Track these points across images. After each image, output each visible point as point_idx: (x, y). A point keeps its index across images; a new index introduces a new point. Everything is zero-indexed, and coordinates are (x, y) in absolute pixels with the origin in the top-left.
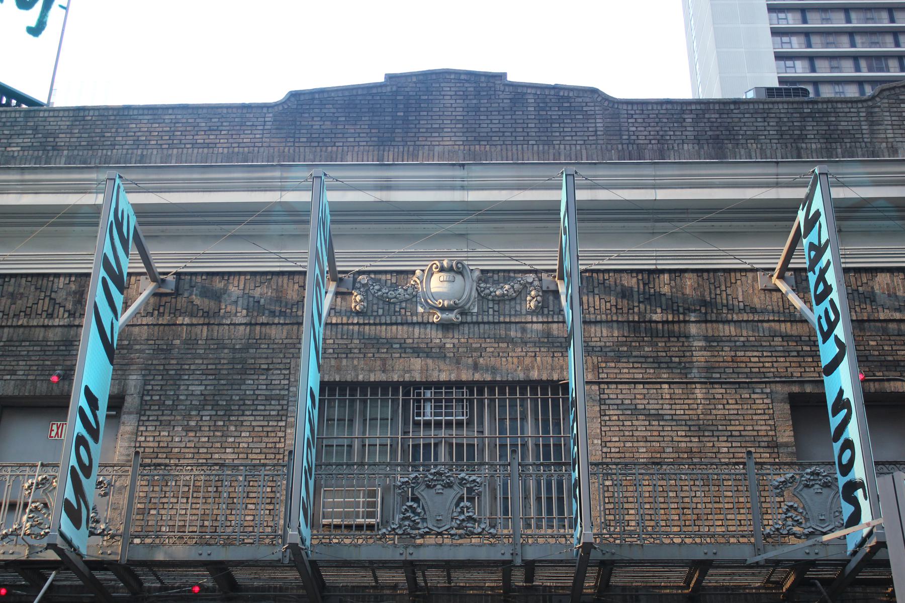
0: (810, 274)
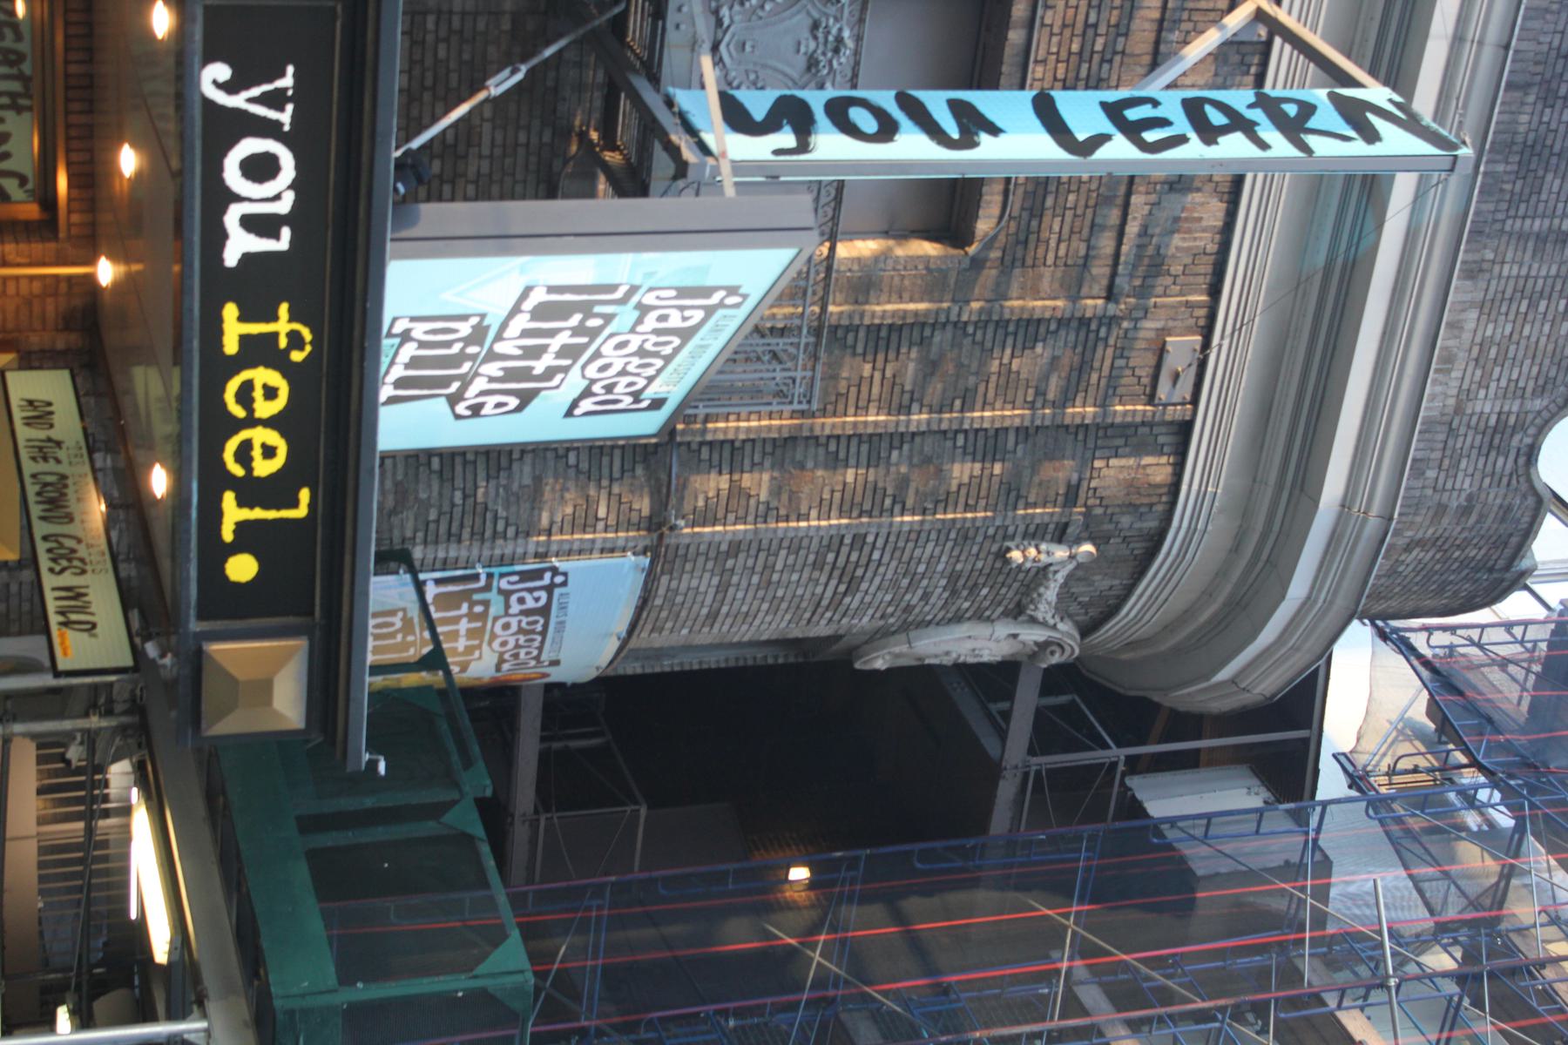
0: (1249, 95)
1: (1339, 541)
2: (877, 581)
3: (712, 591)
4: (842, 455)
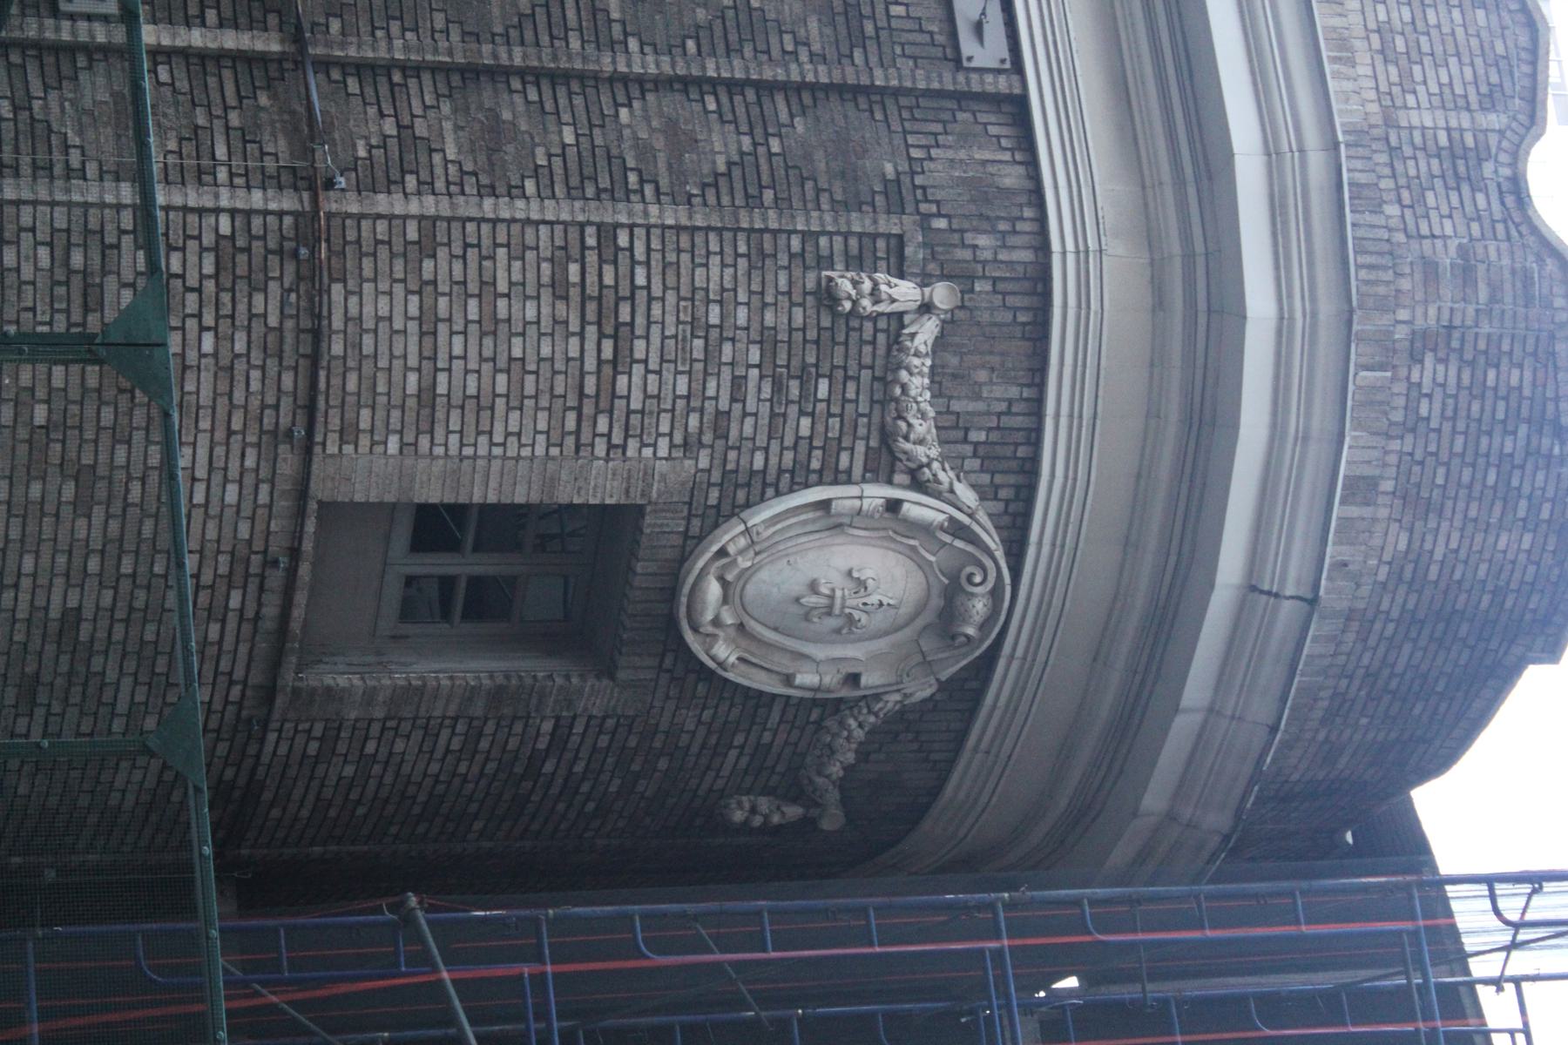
1: (1284, 206)
2: (655, 330)
3: (413, 327)
4: (549, 106)
